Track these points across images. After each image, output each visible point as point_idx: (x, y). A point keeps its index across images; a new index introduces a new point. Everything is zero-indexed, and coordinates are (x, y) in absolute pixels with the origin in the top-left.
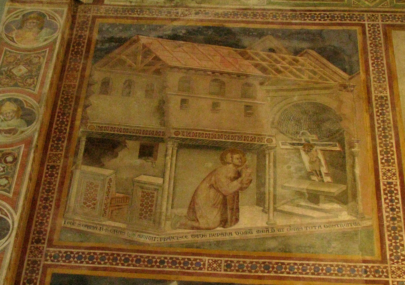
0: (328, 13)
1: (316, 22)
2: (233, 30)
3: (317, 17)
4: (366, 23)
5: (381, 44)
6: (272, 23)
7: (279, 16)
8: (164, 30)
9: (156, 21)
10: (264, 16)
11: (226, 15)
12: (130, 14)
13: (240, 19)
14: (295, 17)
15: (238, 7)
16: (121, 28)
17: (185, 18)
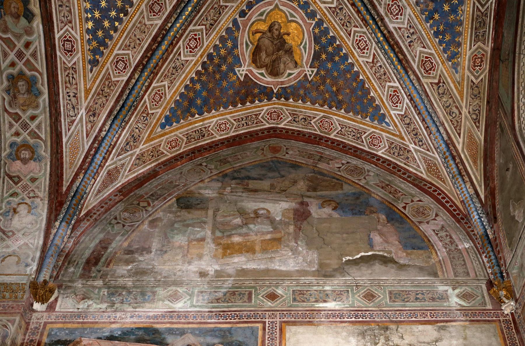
0: (237, 313)
1: (227, 321)
2: (160, 330)
3: (229, 317)
4: (267, 320)
5: (276, 338)
6: (192, 323)
7: (198, 317)
8: (103, 332)
9: (97, 325)
10: (186, 317)
11: (156, 317)
12: (76, 319)
13: (166, 320)
14: (211, 317)
15: (166, 310)
16: (67, 332)
17: (121, 321)
